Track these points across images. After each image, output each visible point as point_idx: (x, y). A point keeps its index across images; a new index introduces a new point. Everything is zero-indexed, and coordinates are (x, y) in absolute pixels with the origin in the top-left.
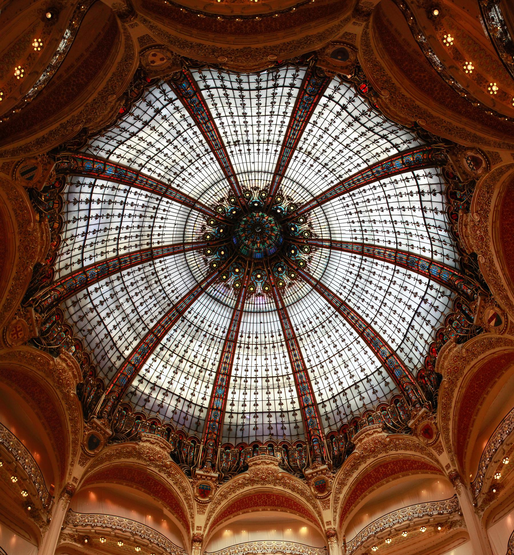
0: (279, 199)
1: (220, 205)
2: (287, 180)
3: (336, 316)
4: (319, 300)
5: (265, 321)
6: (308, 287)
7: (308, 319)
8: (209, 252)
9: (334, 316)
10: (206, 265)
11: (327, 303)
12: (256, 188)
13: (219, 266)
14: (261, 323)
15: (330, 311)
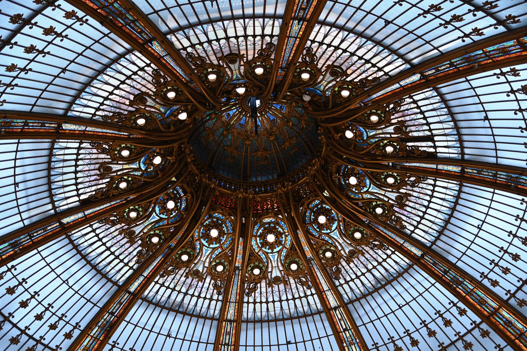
0: (305, 76)
1: (137, 110)
2: (325, 29)
3: (485, 334)
4: (433, 290)
5: (299, 339)
6: (404, 261)
7: (407, 333)
8: (133, 215)
9: (477, 333)
10: (132, 242)
11: (455, 300)
12: (233, 57)
13: (165, 239)
14: (288, 343)
15: (464, 319)
